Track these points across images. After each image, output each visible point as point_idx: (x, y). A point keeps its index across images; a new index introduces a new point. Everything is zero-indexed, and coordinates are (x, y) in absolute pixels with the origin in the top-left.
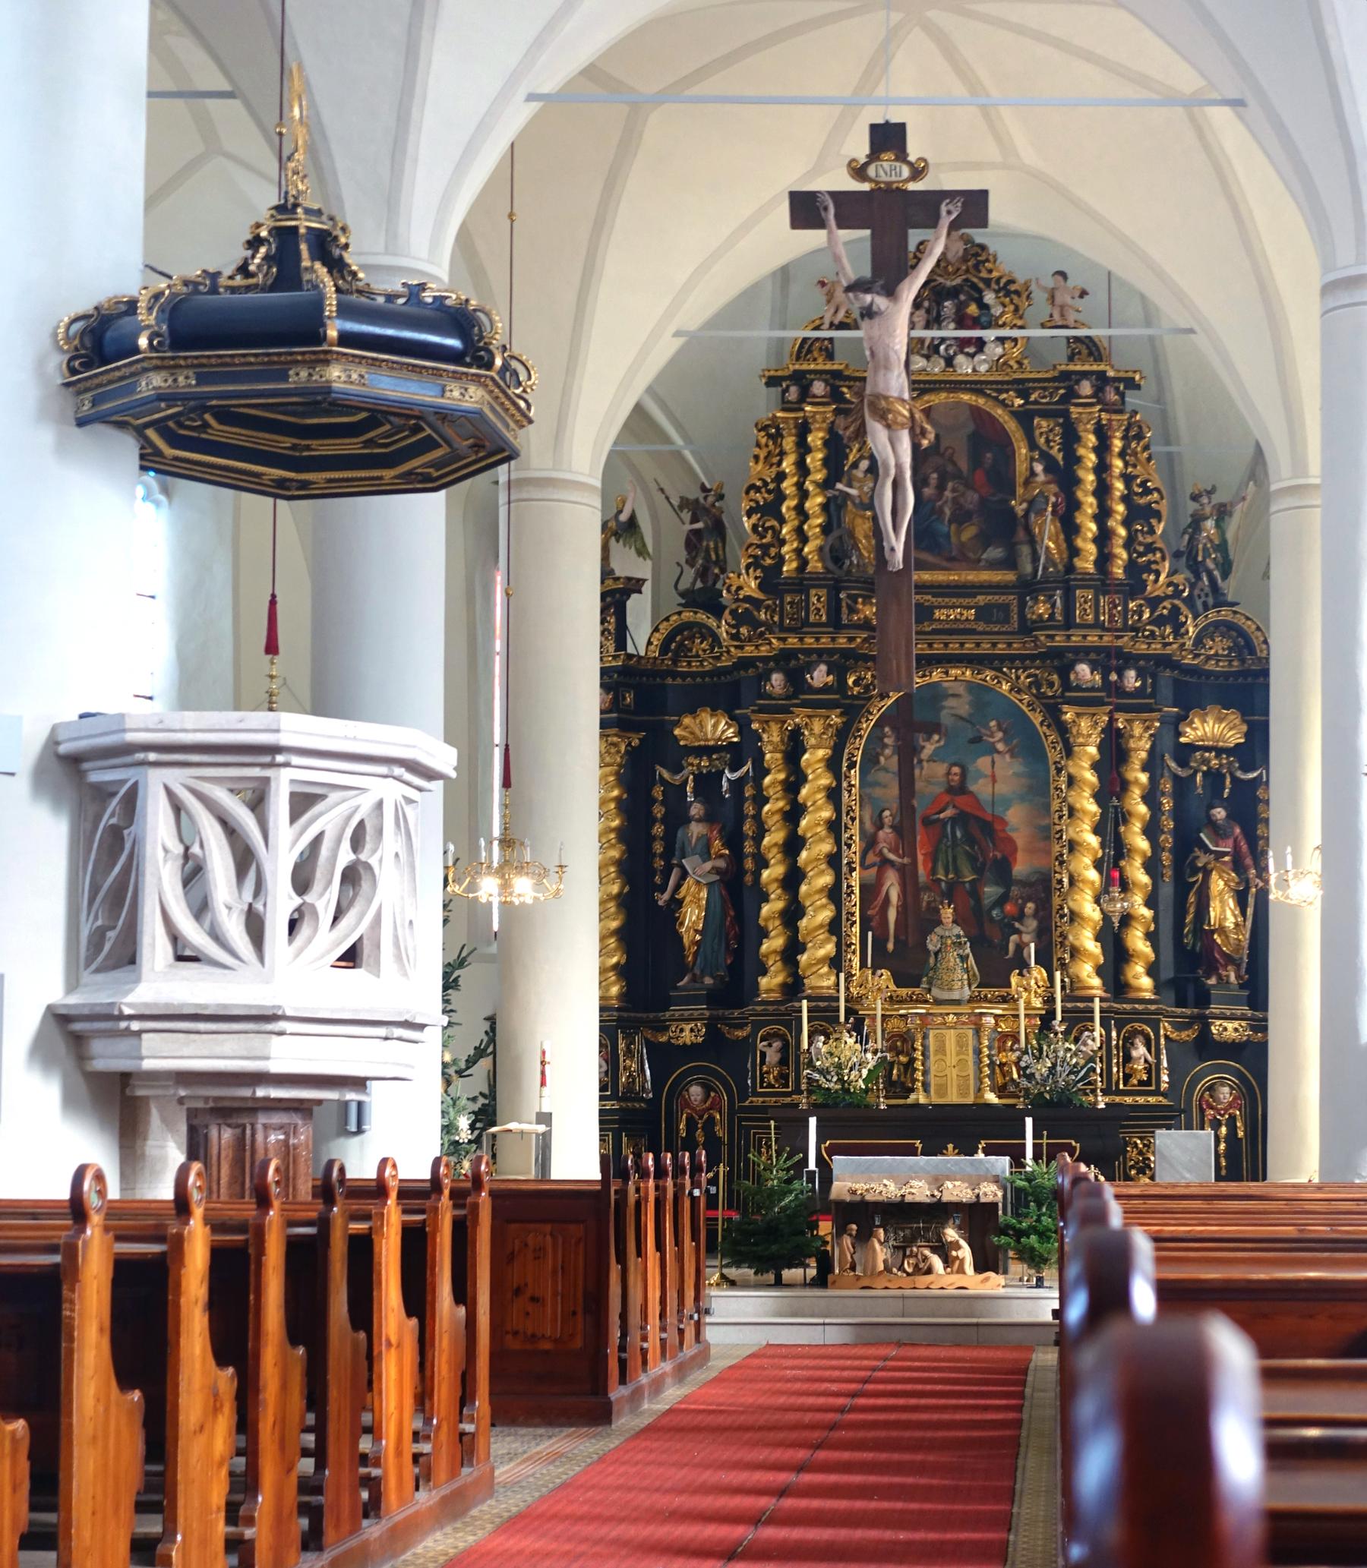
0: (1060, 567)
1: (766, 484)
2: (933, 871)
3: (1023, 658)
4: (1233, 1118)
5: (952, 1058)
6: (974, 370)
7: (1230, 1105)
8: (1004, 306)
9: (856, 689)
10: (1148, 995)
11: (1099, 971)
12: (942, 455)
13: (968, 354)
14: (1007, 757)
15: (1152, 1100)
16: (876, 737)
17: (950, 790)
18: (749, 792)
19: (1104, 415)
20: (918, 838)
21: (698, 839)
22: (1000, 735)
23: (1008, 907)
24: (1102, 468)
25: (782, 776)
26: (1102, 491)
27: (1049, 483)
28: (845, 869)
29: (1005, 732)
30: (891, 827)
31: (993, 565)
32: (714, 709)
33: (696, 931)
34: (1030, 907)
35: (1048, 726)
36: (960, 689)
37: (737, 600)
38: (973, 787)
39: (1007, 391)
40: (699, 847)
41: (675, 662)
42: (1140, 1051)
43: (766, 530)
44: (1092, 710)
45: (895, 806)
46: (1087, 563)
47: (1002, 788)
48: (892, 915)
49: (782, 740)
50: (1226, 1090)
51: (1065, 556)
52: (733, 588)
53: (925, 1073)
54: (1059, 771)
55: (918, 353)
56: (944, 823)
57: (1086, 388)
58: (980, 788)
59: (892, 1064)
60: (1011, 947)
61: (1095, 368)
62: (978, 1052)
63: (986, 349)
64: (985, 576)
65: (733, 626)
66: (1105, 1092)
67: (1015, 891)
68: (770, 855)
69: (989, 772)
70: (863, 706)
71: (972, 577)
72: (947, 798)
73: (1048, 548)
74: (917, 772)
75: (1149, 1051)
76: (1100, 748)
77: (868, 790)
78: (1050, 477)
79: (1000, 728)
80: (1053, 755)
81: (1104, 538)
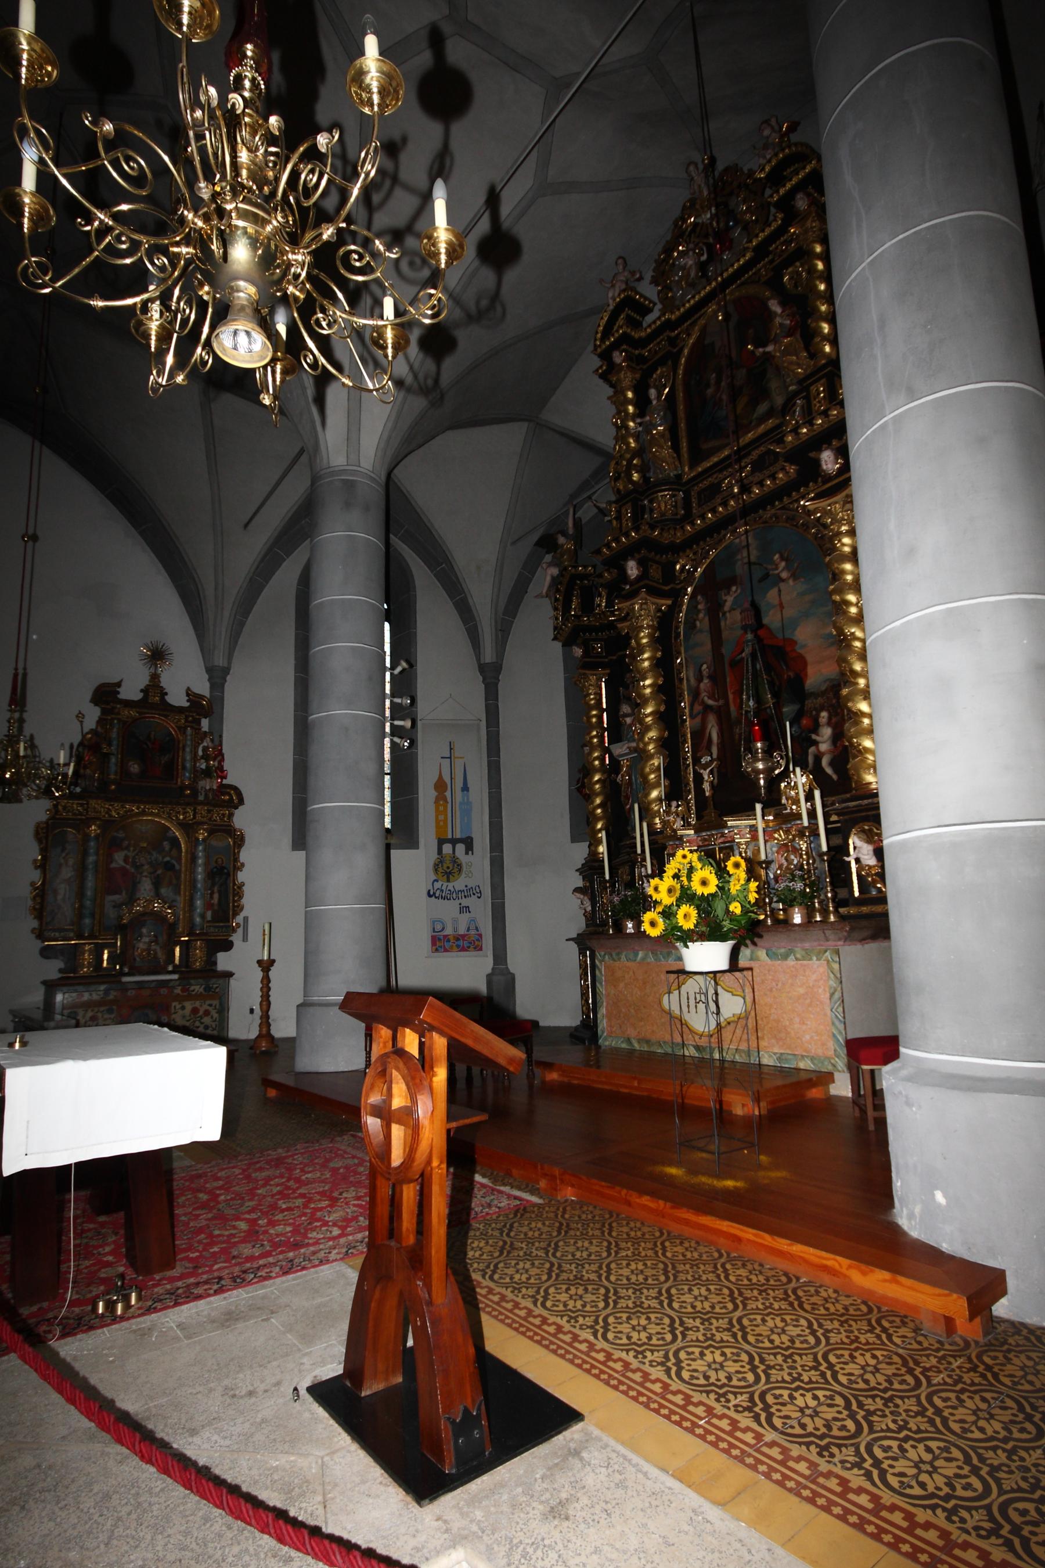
14: (791, 582)
20: (728, 680)
30: (708, 677)
47: (788, 613)
69: (776, 602)
74: (722, 624)
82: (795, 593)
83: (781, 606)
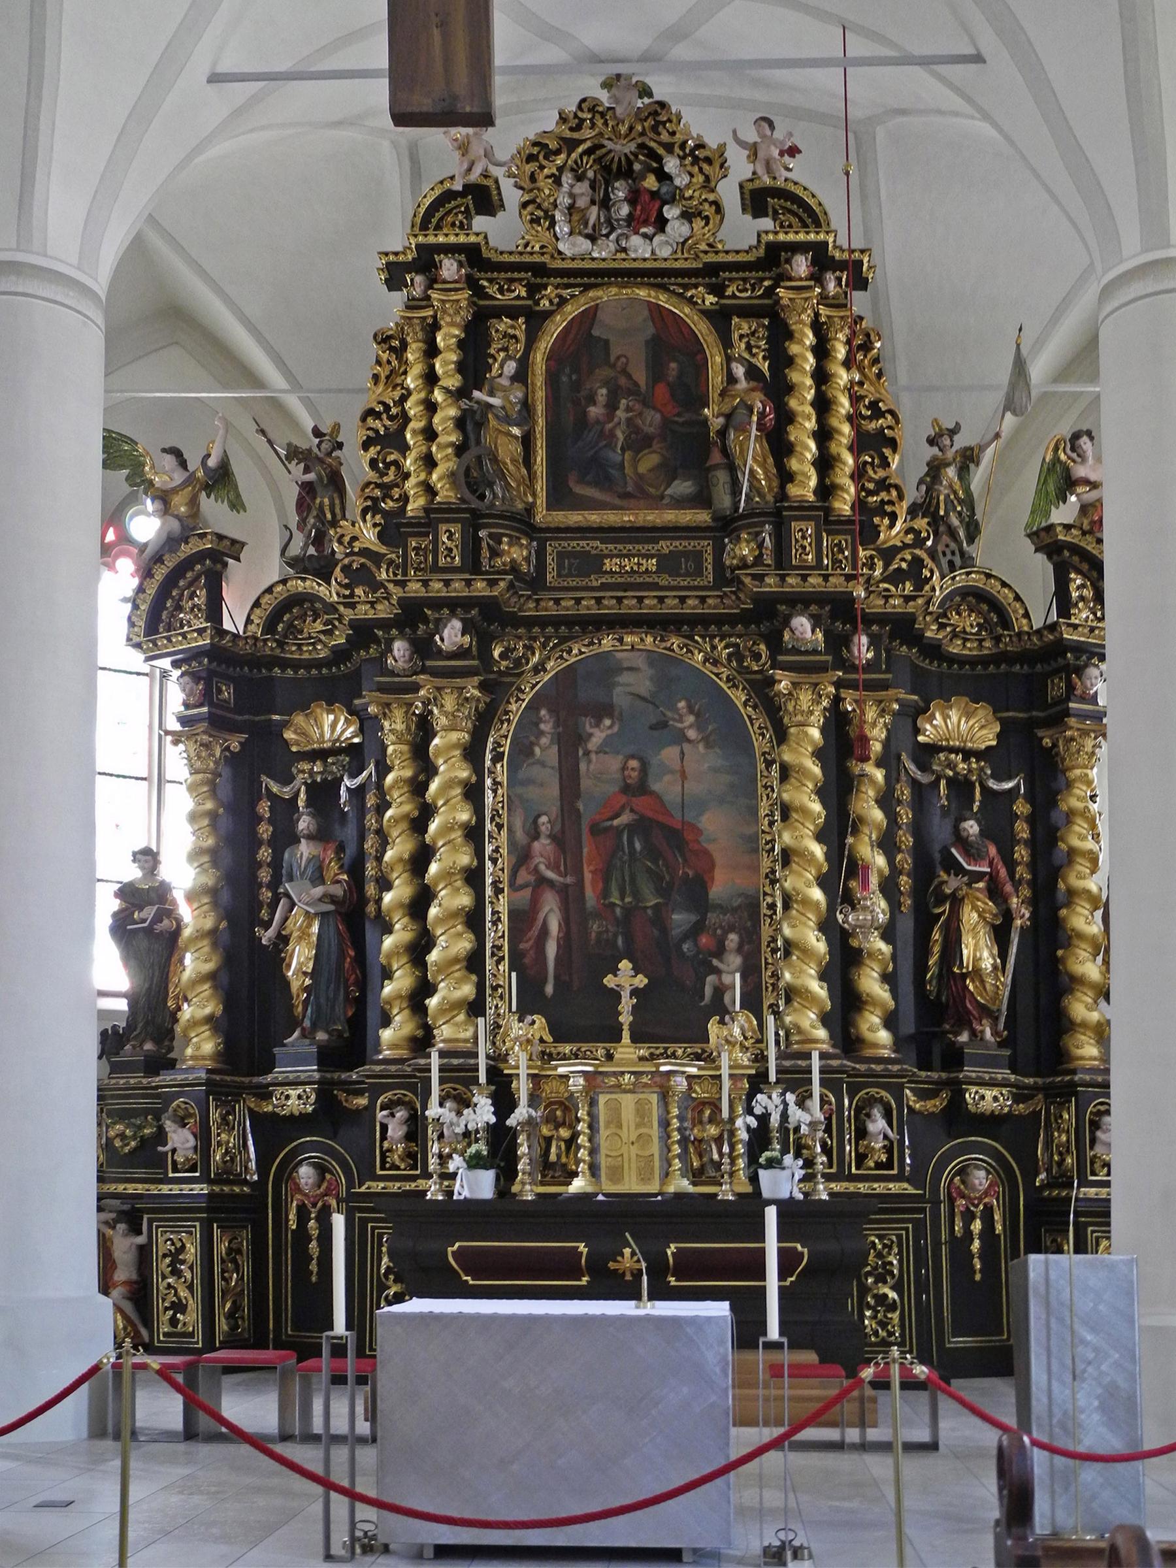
0: (770, 498)
1: (387, 408)
2: (606, 893)
3: (719, 620)
4: (989, 1210)
5: (629, 1132)
6: (653, 253)
7: (986, 1193)
8: (692, 175)
9: (504, 663)
10: (886, 1053)
11: (825, 1020)
12: (613, 366)
13: (645, 236)
14: (701, 747)
15: (894, 1187)
16: (530, 721)
17: (626, 789)
18: (371, 800)
19: (823, 310)
20: (585, 850)
21: (309, 861)
22: (691, 719)
23: (704, 940)
24: (821, 377)
25: (408, 773)
26: (823, 405)
27: (753, 390)
28: (489, 891)
29: (698, 715)
30: (549, 836)
31: (680, 503)
32: (330, 703)
33: (305, 973)
34: (733, 938)
35: (755, 707)
36: (640, 661)
37: (352, 553)
38: (656, 787)
39: (696, 286)
40: (309, 871)
41: (281, 644)
42: (877, 1124)
43: (388, 466)
44: (814, 678)
45: (555, 810)
46: (806, 487)
47: (693, 787)
48: (551, 950)
49: (408, 728)
50: (982, 1174)
51: (775, 484)
52: (347, 539)
53: (593, 1152)
54: (769, 764)
55: (580, 233)
56: (619, 831)
57: (801, 266)
58: (666, 787)
59: (548, 1140)
60: (708, 991)
61: (812, 237)
62: (665, 1124)
63: (668, 228)
64: (670, 516)
65: (346, 586)
66: (828, 1178)
67: (712, 918)
68: (395, 875)
69: (677, 765)
70: (512, 684)
71: (652, 517)
72: (623, 799)
73: (752, 471)
74: (583, 766)
75: (890, 1124)
76: (823, 731)
77: (519, 790)
78: (753, 384)
79: (691, 710)
80: (760, 744)
81: (825, 463)
82: (706, 765)
83: (683, 775)
